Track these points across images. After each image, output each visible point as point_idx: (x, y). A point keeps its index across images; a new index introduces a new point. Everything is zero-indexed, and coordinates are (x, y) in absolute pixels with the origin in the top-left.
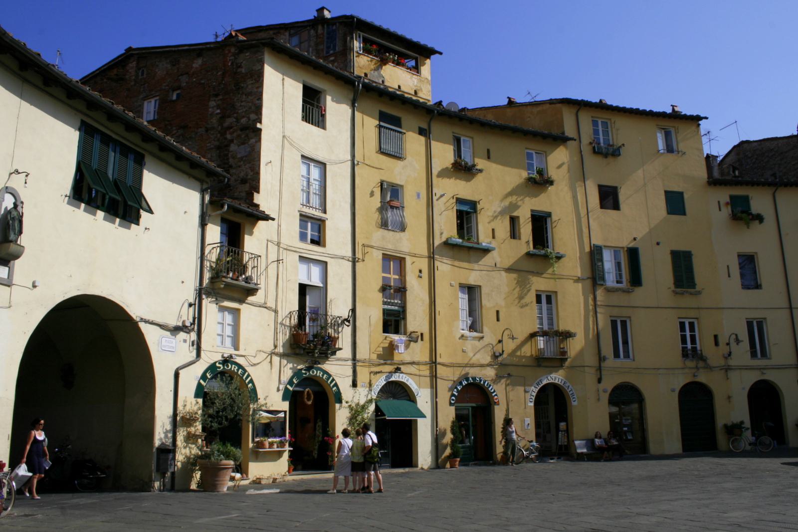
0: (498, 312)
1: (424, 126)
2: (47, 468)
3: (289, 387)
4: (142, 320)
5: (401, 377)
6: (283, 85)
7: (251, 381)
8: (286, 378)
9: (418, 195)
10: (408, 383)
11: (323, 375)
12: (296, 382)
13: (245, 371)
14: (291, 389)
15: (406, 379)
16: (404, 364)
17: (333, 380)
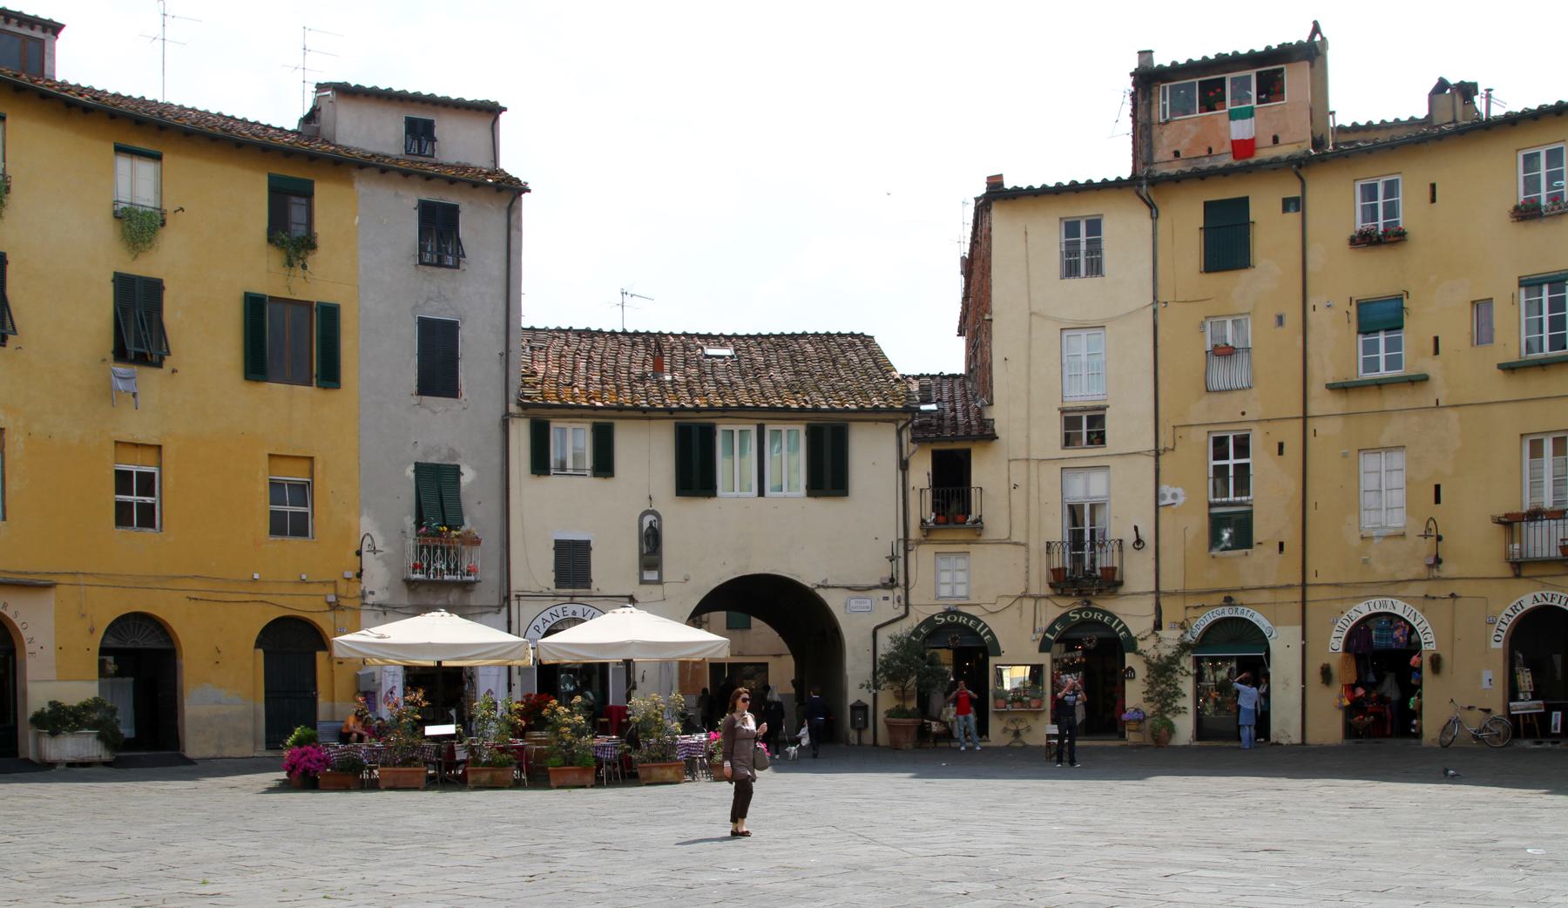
0: (1437, 488)
1: (1295, 192)
2: (765, 724)
3: (1047, 635)
4: (819, 586)
5: (1239, 611)
6: (1026, 241)
7: (990, 632)
8: (1044, 624)
9: (1280, 320)
10: (1253, 620)
11: (1103, 618)
12: (1059, 629)
13: (979, 621)
14: (1052, 638)
15: (1249, 614)
16: (1243, 589)
17: (1120, 622)
